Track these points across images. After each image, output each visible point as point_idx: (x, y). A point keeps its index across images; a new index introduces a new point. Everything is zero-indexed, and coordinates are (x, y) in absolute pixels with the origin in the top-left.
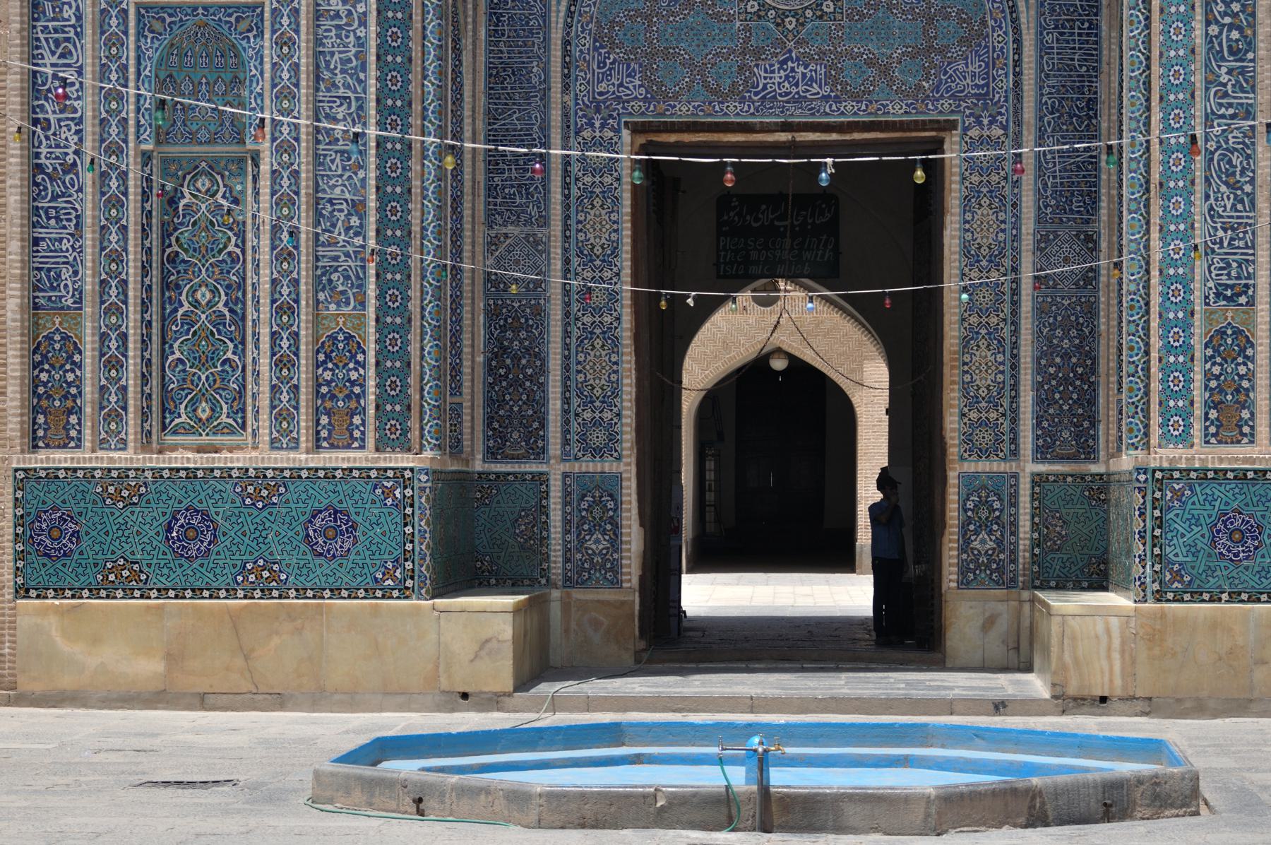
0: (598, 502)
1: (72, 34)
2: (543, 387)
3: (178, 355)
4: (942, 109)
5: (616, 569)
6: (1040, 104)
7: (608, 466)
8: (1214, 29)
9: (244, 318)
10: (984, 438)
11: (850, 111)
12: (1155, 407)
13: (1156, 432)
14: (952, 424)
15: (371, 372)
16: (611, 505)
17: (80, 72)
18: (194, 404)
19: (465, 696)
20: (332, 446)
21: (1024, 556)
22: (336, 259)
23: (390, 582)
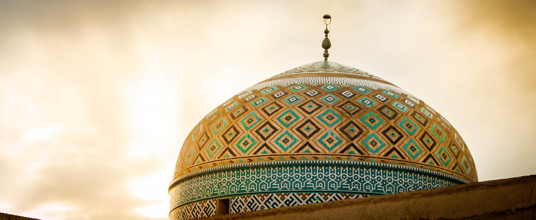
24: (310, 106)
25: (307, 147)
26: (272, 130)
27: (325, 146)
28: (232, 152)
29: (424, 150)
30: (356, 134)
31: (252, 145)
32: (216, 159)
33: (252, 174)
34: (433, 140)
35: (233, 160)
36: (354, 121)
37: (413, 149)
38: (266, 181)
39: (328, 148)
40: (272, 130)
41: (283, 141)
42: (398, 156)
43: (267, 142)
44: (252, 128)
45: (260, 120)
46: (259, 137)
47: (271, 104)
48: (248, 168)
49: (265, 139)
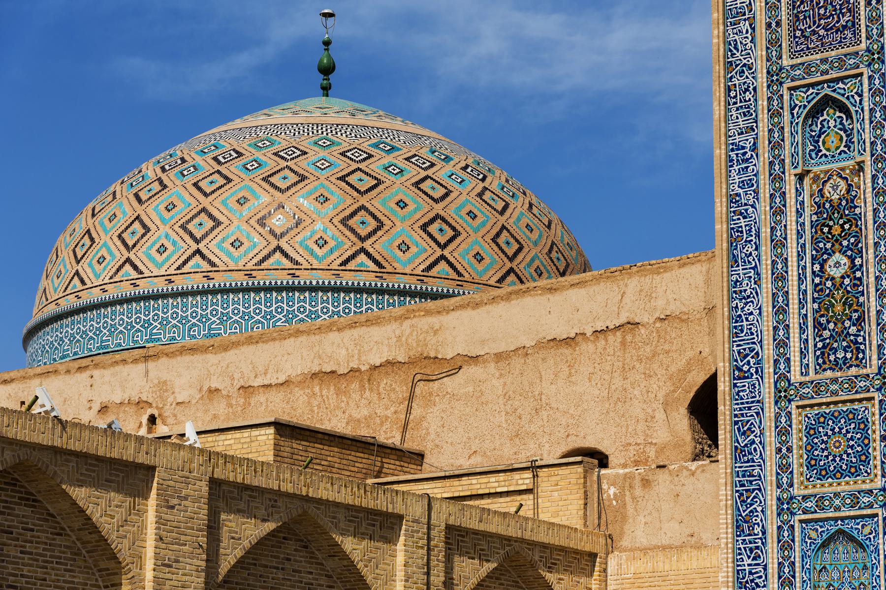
1: (760, 544)
24: (285, 178)
25: (278, 254)
26: (211, 224)
27: (312, 253)
28: (135, 268)
29: (499, 258)
30: (370, 229)
31: (174, 252)
32: (107, 280)
33: (173, 306)
34: (517, 241)
35: (138, 282)
36: (368, 205)
37: (478, 257)
38: (199, 320)
39: (317, 257)
40: (211, 224)
41: (232, 244)
42: (451, 271)
43: (201, 246)
44: (174, 221)
45: (190, 204)
46: (187, 237)
47: (211, 174)
48: (164, 296)
49: (197, 241)
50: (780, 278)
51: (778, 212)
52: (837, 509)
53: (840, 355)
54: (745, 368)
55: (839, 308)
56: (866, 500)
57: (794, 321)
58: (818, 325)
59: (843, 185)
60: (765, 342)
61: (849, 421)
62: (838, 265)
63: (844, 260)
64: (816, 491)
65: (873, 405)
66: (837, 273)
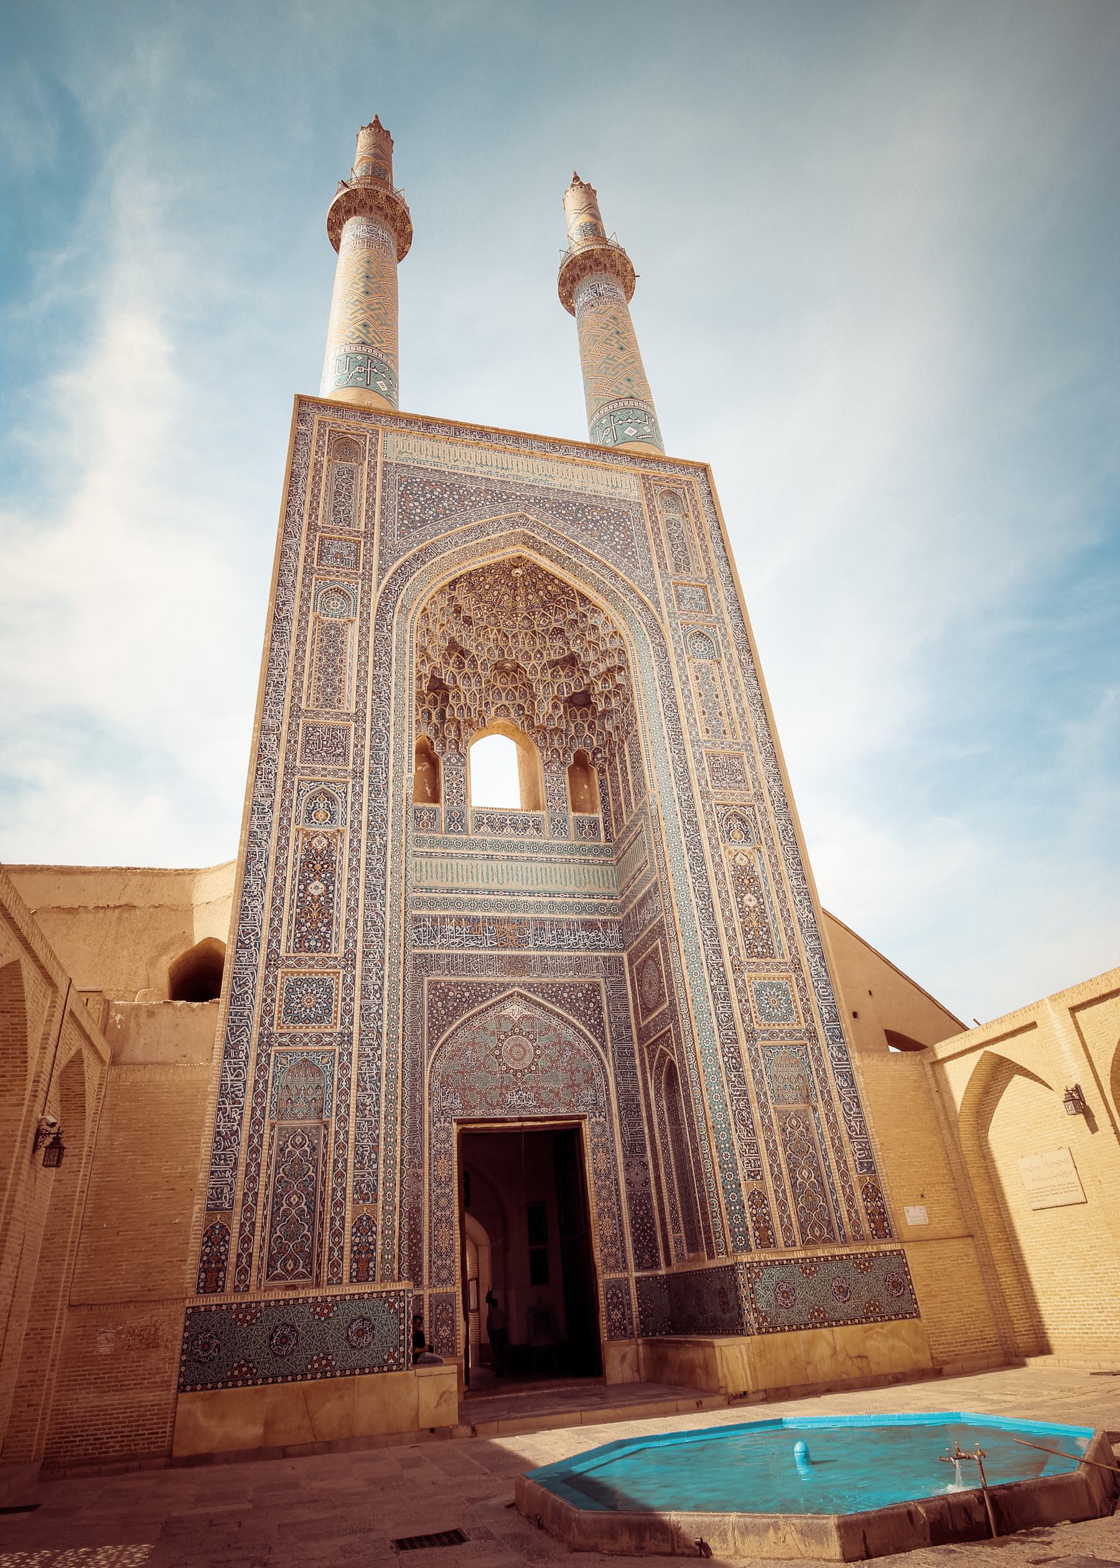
0: (445, 1309)
2: (421, 1249)
3: (279, 1234)
4: (580, 1110)
5: (453, 1346)
6: (619, 1107)
7: (449, 1289)
8: (726, 1059)
9: (314, 1212)
10: (611, 1261)
11: (545, 1112)
12: (727, 1232)
13: (730, 1246)
14: (597, 1255)
15: (380, 1237)
16: (450, 1310)
17: (245, 1083)
18: (285, 1261)
19: (432, 1430)
20: (358, 1281)
21: (636, 1321)
22: (363, 1176)
23: (391, 1361)
50: (279, 888)
51: (282, 848)
52: (306, 1044)
53: (313, 943)
54: (247, 942)
55: (315, 914)
56: (327, 1039)
57: (285, 917)
58: (298, 922)
59: (325, 842)
60: (264, 927)
61: (319, 986)
62: (316, 888)
63: (321, 886)
64: (290, 1031)
65: (338, 978)
66: (316, 893)
